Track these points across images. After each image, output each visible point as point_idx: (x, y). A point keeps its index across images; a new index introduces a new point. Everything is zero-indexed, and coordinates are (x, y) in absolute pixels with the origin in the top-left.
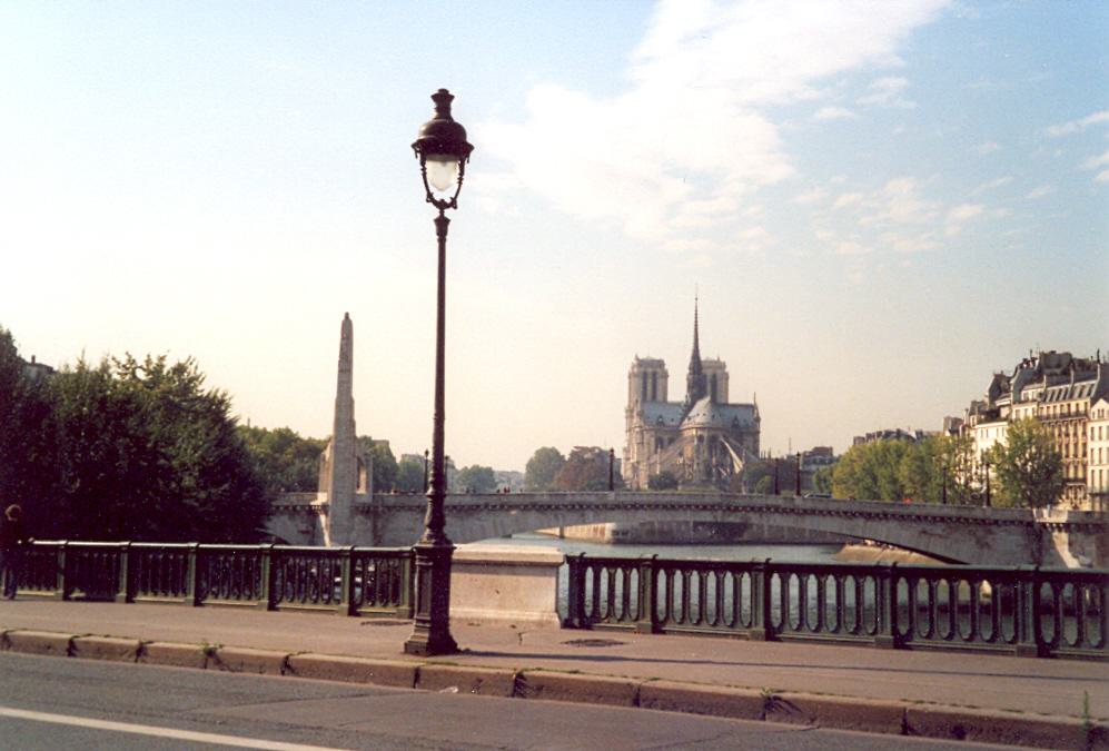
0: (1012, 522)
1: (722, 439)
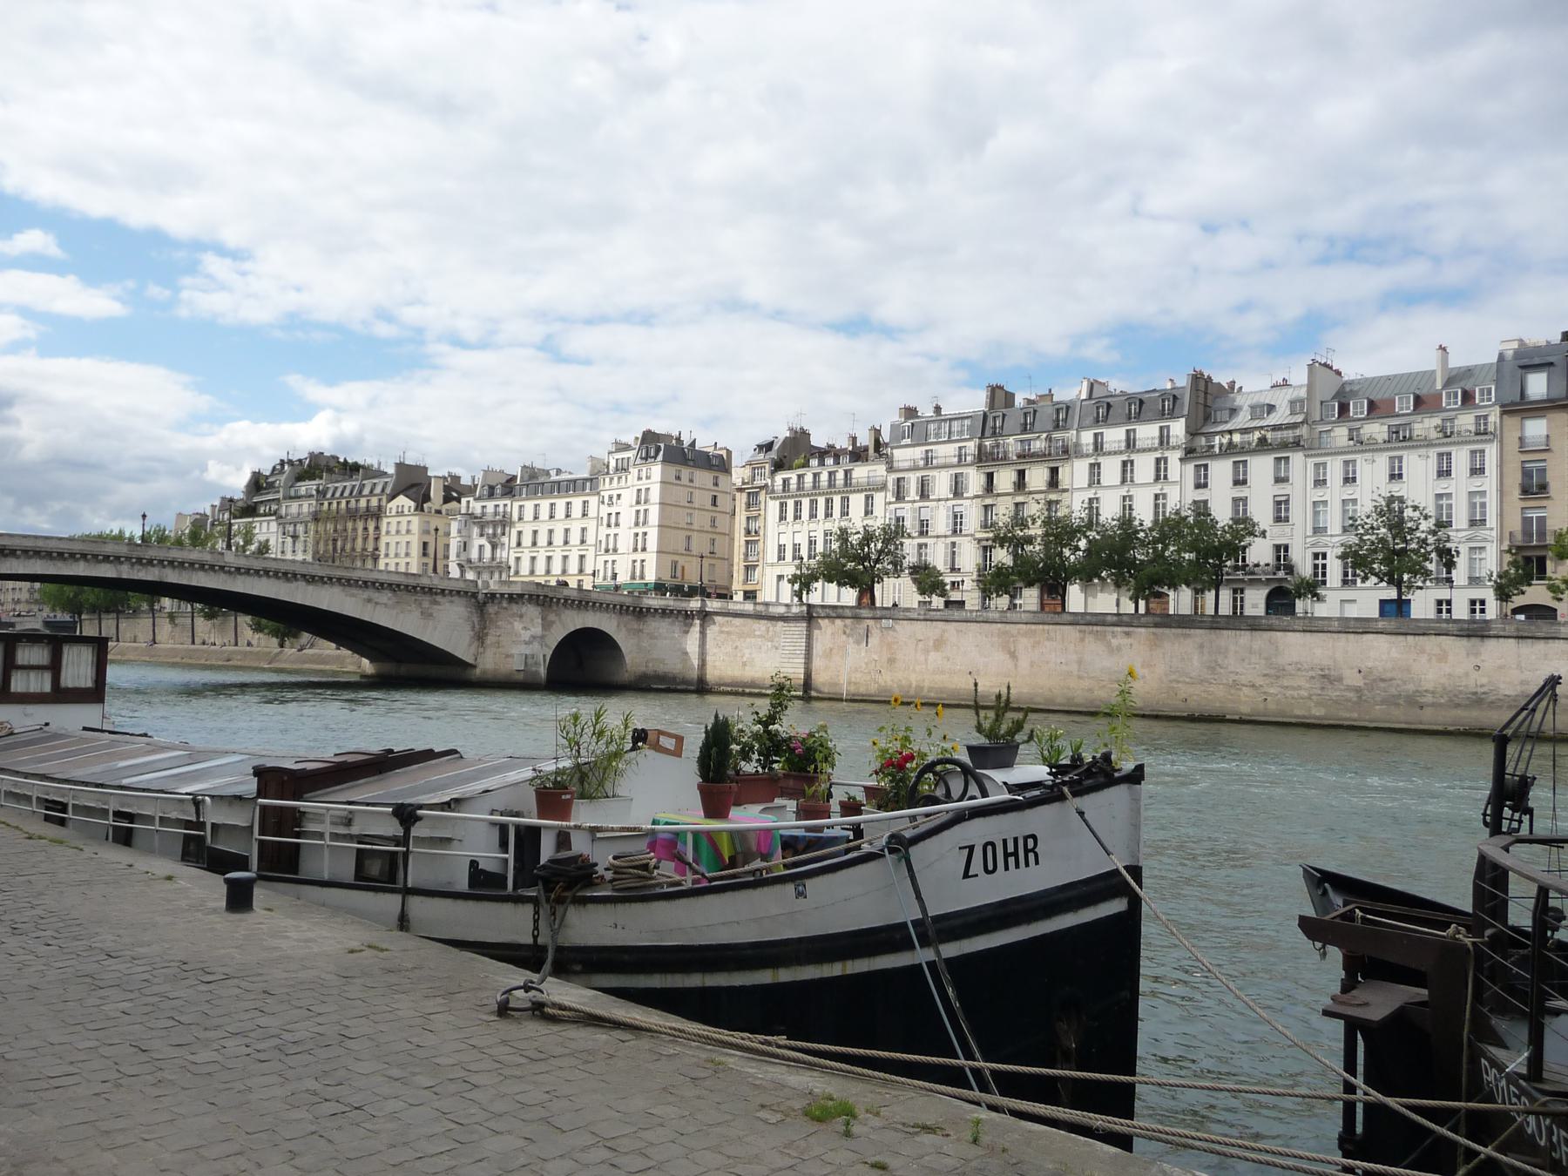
0: (458, 592)
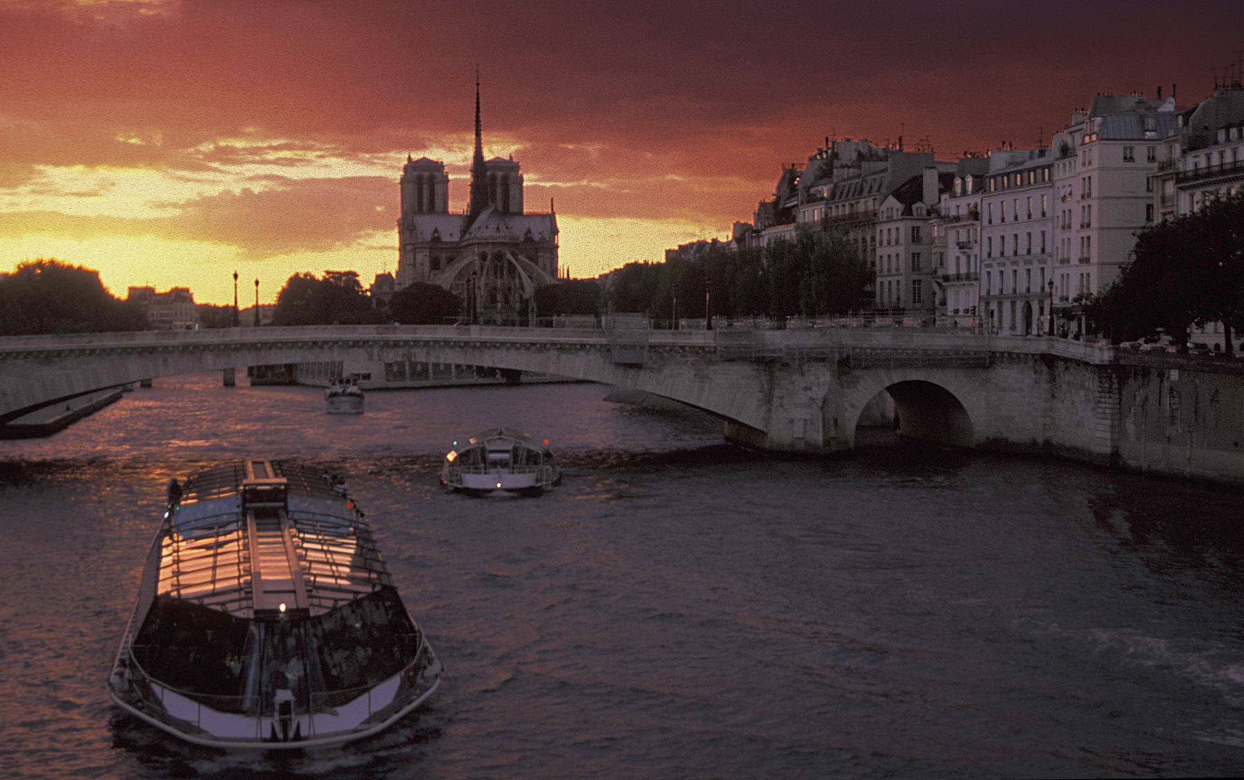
1: (509, 256)
